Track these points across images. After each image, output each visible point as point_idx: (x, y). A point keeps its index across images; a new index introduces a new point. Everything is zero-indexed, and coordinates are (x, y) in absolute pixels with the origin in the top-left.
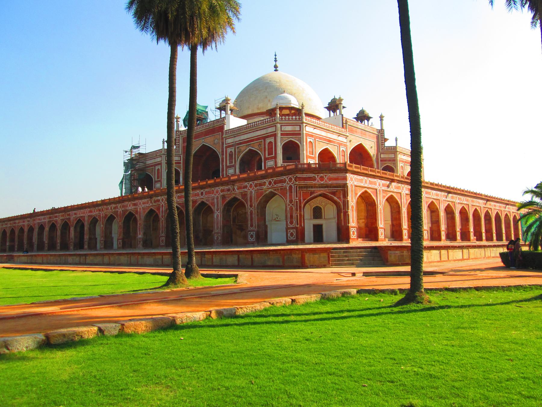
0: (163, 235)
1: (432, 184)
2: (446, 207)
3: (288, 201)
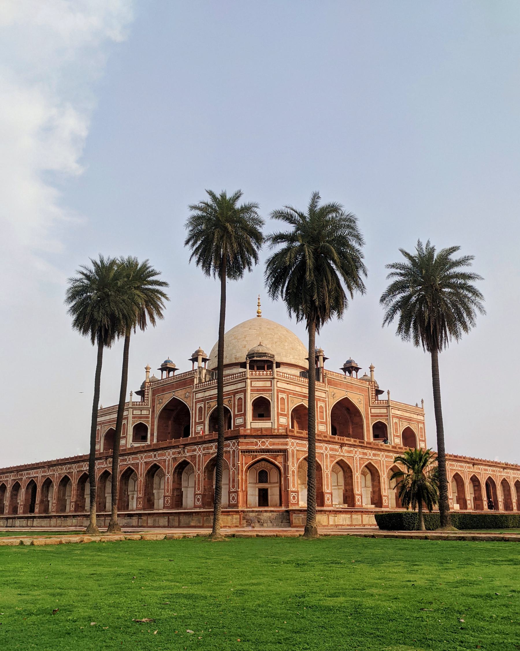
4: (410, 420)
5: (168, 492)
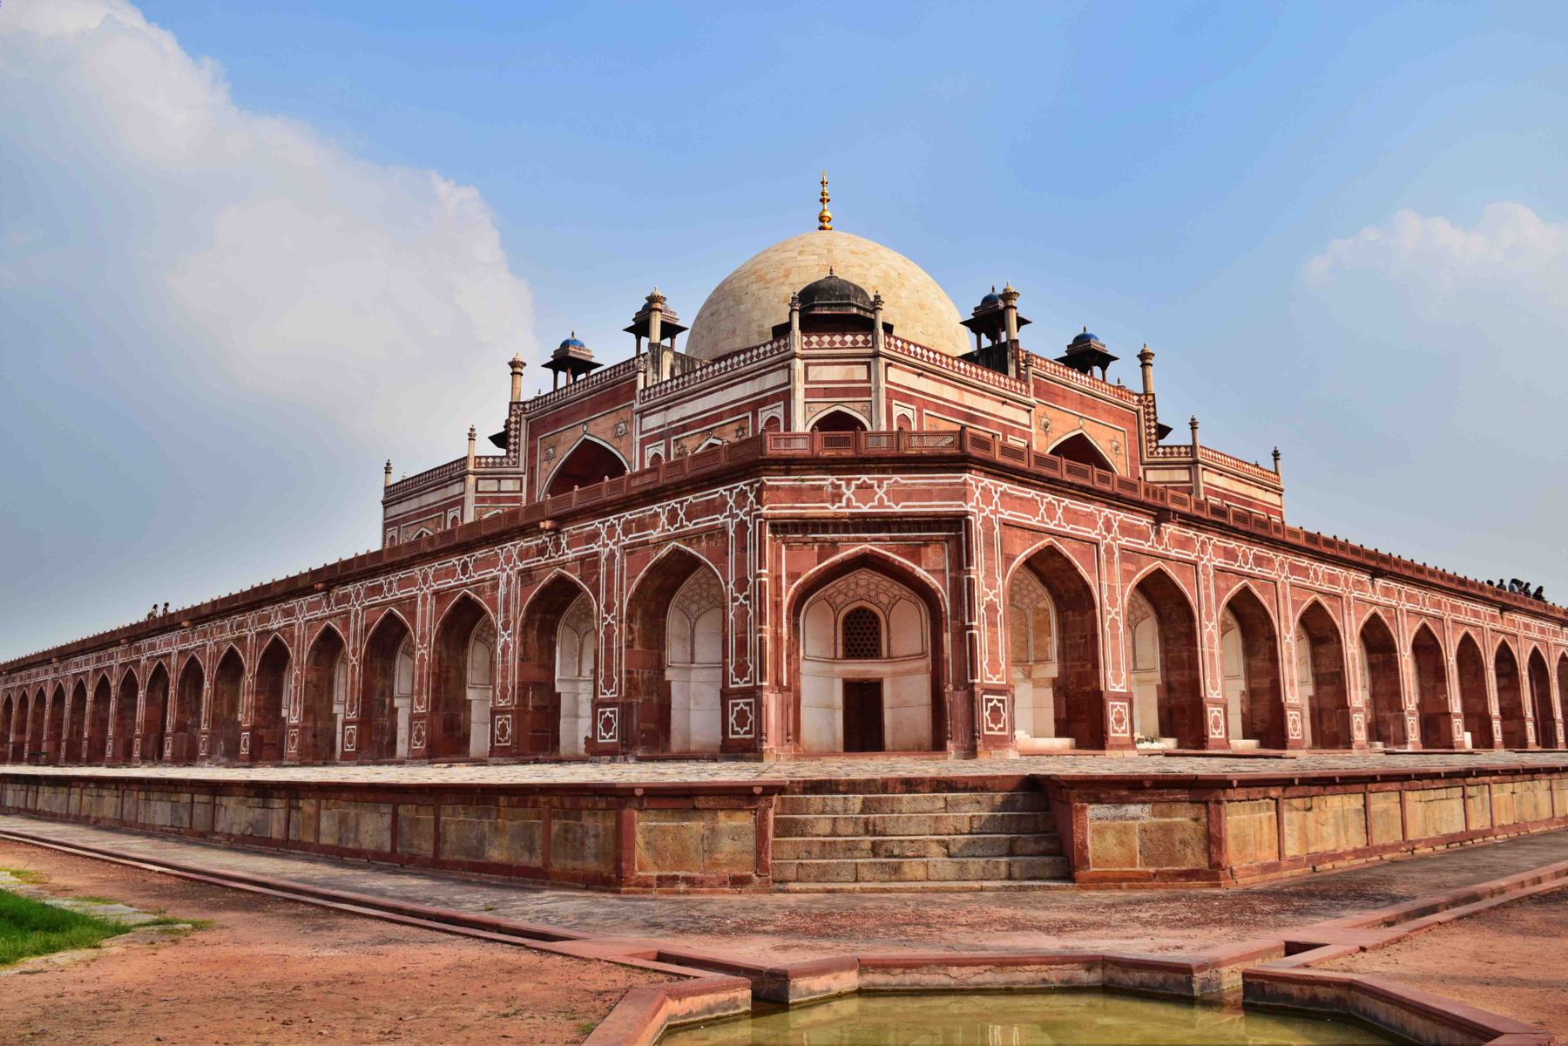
0: (352, 716)
1: (1312, 538)
2: (1367, 625)
3: (731, 585)
4: (1250, 504)
5: (504, 696)
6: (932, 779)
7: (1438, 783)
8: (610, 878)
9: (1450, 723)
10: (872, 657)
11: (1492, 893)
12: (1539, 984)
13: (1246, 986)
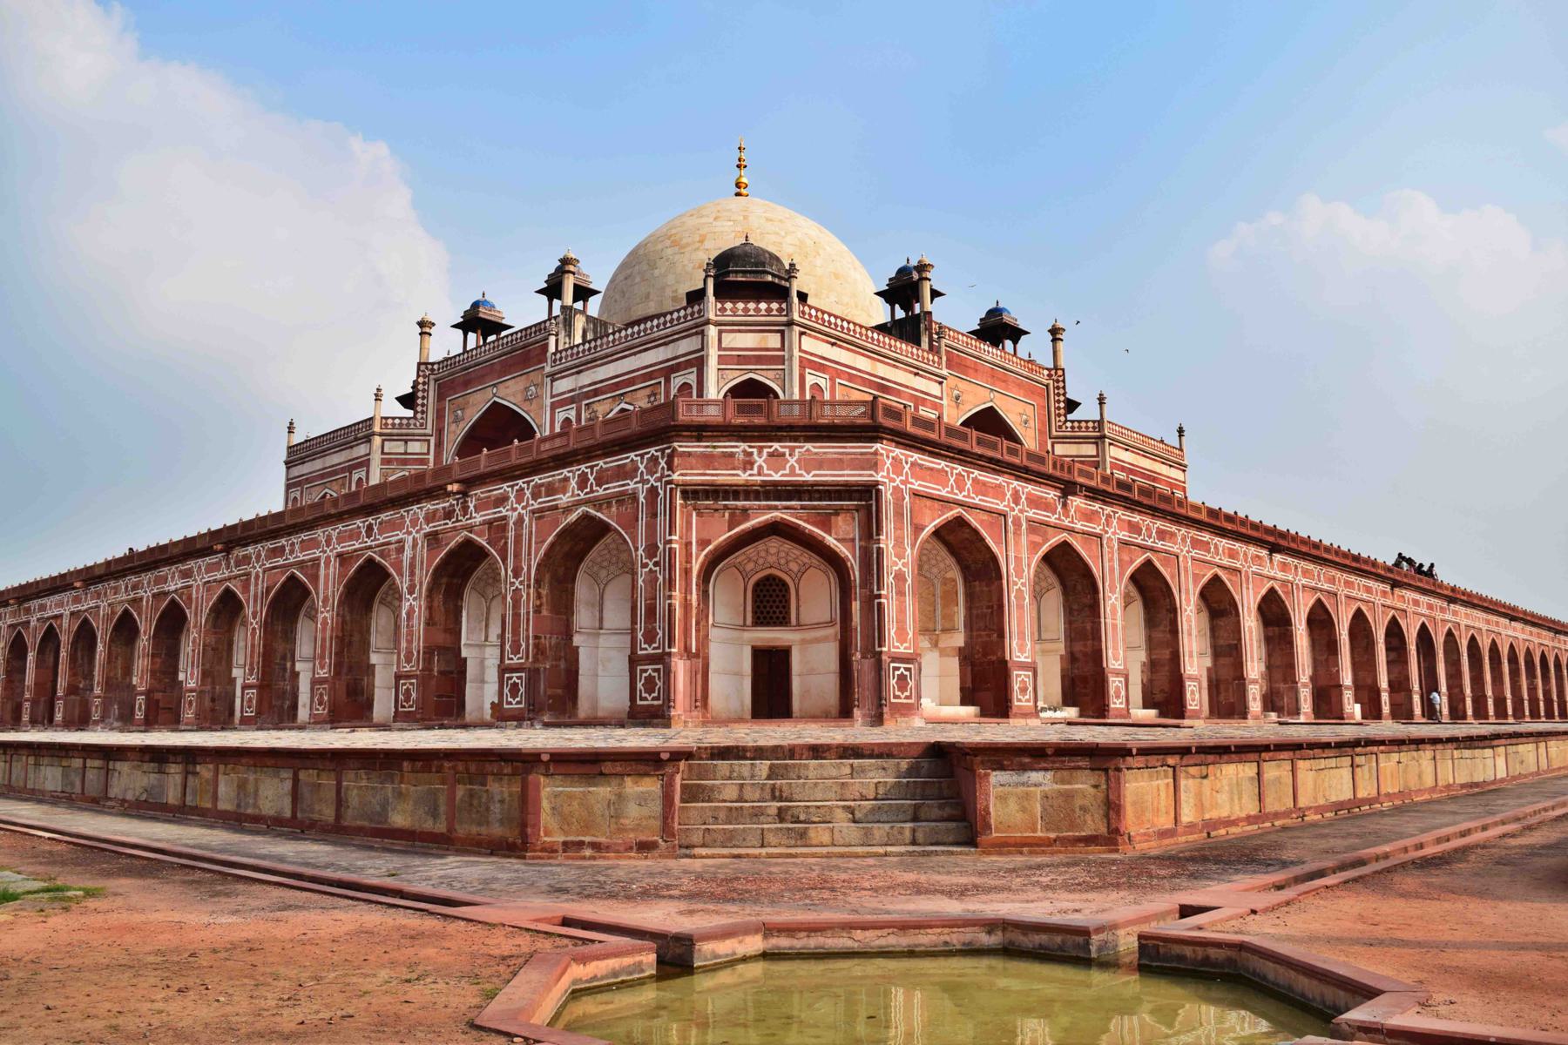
0: (252, 680)
1: (1214, 513)
2: (1264, 598)
4: (1155, 480)
5: (408, 661)
6: (839, 746)
7: (1328, 752)
8: (515, 843)
9: (1341, 694)
10: (781, 624)
11: (1377, 858)
12: (1419, 944)
13: (1141, 947)
